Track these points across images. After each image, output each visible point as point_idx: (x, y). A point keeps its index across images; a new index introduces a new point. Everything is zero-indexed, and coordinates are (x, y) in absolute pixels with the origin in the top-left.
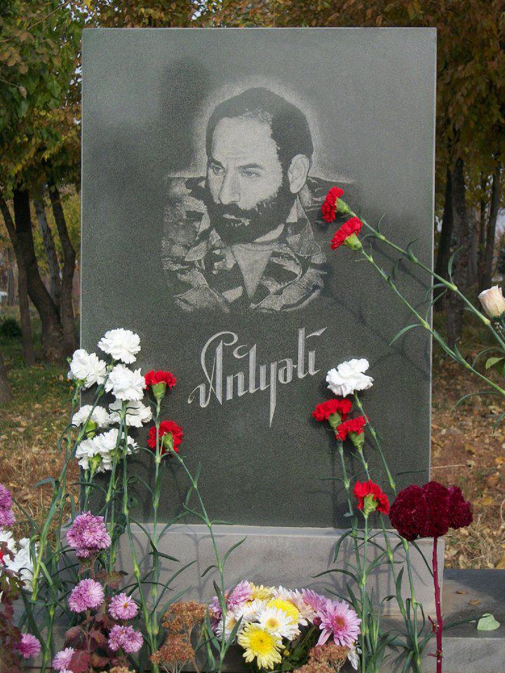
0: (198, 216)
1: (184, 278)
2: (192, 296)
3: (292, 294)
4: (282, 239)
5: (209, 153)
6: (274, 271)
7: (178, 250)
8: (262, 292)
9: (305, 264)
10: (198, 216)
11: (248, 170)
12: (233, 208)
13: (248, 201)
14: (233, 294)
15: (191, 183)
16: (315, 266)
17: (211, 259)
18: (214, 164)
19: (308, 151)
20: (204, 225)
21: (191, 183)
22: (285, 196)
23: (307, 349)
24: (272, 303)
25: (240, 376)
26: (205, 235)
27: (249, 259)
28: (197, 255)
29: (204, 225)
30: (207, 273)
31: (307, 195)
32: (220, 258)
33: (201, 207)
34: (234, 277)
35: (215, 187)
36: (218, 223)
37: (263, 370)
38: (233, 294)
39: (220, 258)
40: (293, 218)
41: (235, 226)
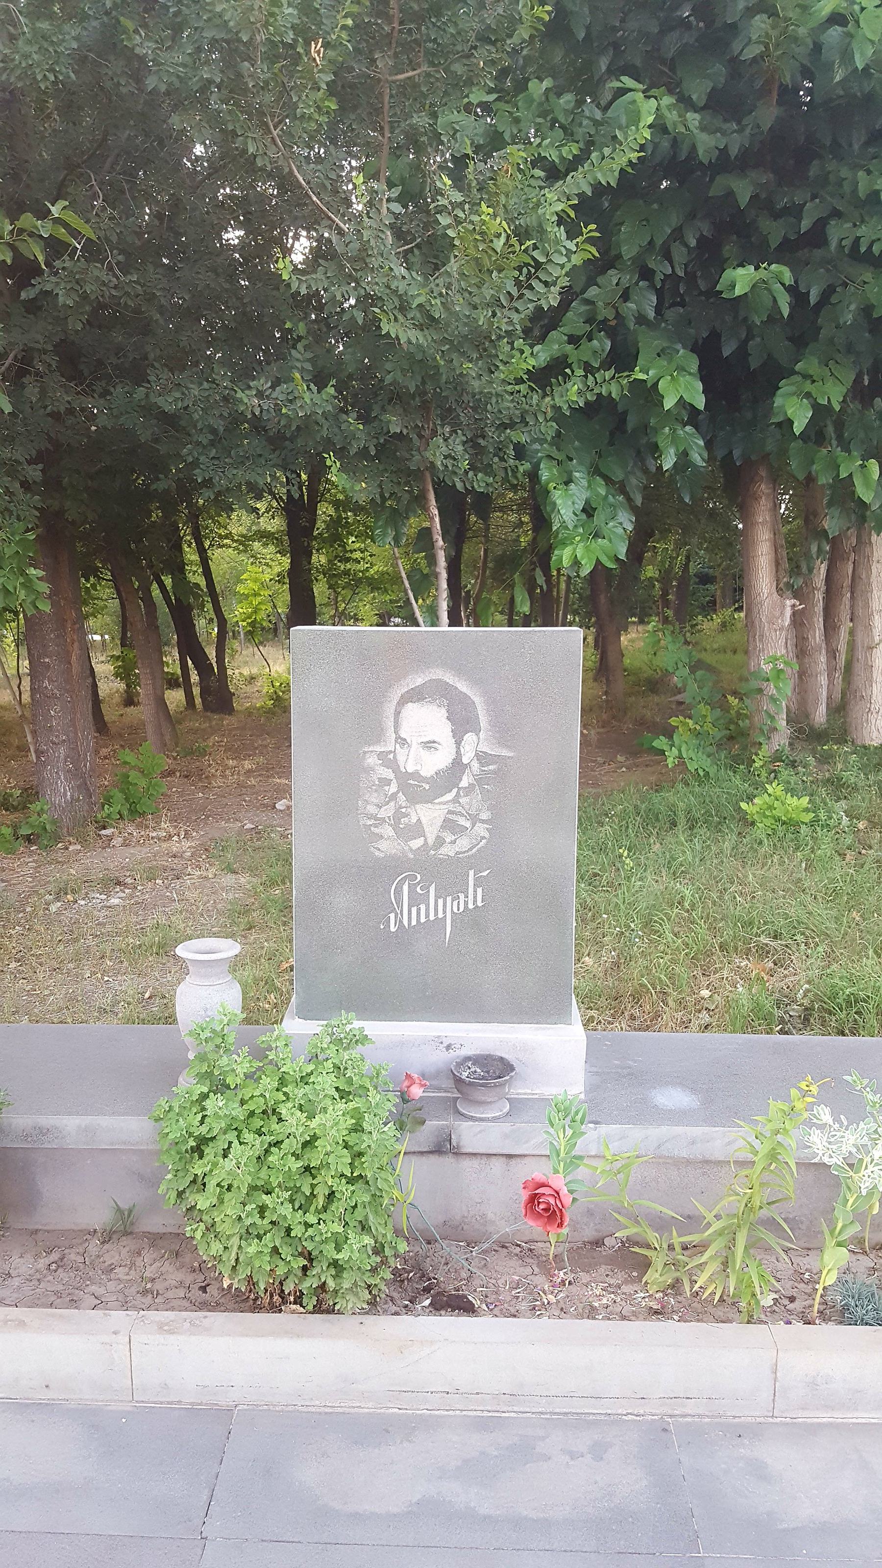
0: (388, 782)
1: (376, 830)
2: (384, 845)
3: (463, 843)
4: (455, 800)
5: (396, 732)
6: (449, 825)
7: (371, 809)
8: (440, 842)
9: (475, 819)
10: (388, 782)
11: (430, 745)
12: (416, 775)
13: (428, 771)
14: (417, 843)
15: (381, 755)
16: (483, 822)
17: (399, 815)
18: (402, 741)
19: (477, 731)
20: (393, 788)
21: (381, 755)
22: (458, 766)
23: (476, 886)
24: (447, 850)
25: (423, 907)
26: (394, 797)
27: (430, 816)
28: (387, 812)
29: (393, 788)
30: (395, 827)
31: (475, 765)
32: (407, 815)
33: (388, 774)
34: (418, 830)
35: (401, 759)
36: (403, 787)
37: (441, 902)
38: (417, 843)
39: (407, 815)
40: (464, 783)
41: (415, 789)
